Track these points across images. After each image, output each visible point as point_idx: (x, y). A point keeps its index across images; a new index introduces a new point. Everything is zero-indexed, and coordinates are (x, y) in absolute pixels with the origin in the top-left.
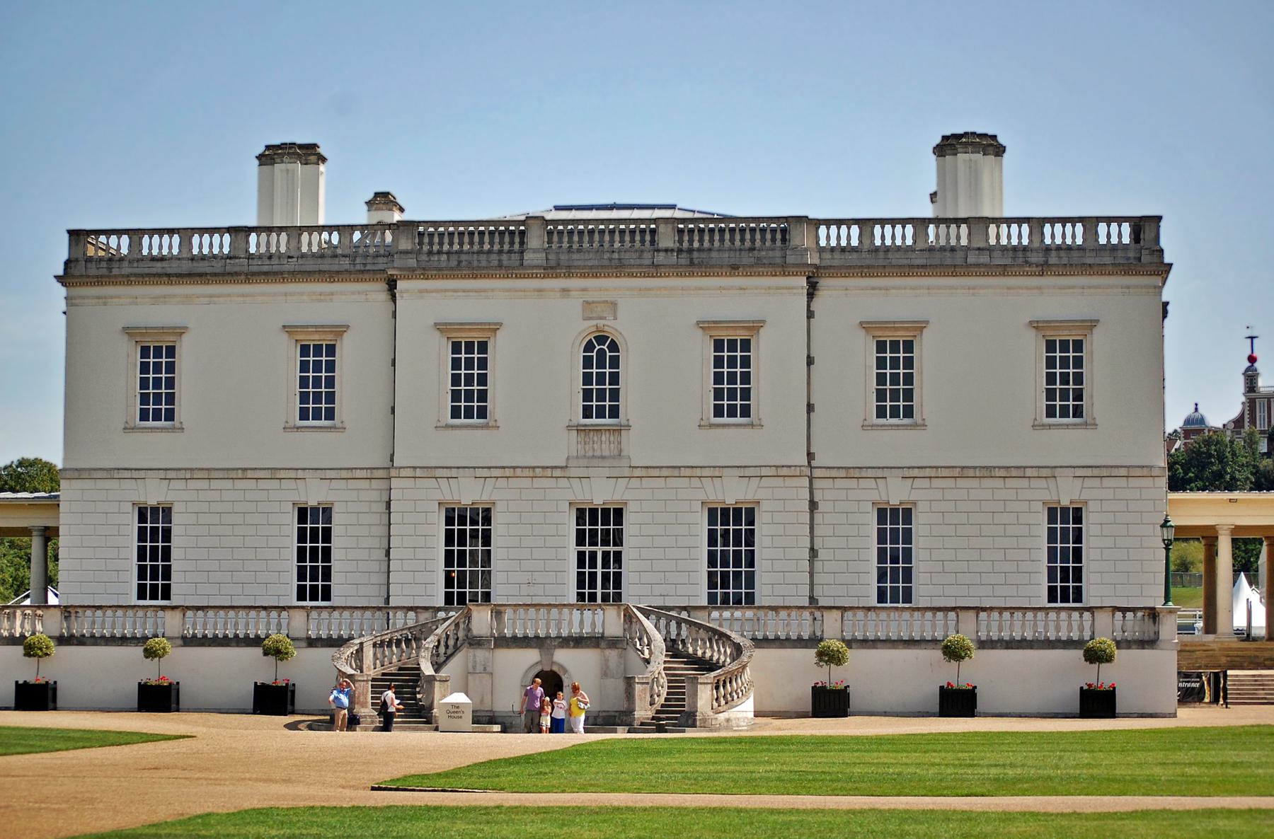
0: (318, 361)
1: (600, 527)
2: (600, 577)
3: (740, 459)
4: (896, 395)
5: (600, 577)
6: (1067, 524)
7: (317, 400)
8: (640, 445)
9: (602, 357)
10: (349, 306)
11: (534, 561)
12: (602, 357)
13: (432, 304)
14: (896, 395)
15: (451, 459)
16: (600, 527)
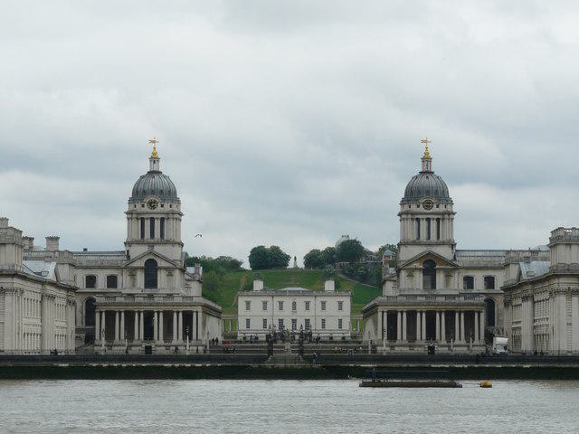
0: (265, 304)
1: (294, 321)
2: (294, 327)
3: (308, 315)
4: (323, 308)
5: (294, 327)
6: (340, 321)
7: (265, 308)
8: (299, 313)
9: (294, 304)
10: (269, 299)
11: (288, 326)
12: (294, 304)
13: (277, 299)
14: (323, 308)
15: (279, 314)
16: (294, 321)
